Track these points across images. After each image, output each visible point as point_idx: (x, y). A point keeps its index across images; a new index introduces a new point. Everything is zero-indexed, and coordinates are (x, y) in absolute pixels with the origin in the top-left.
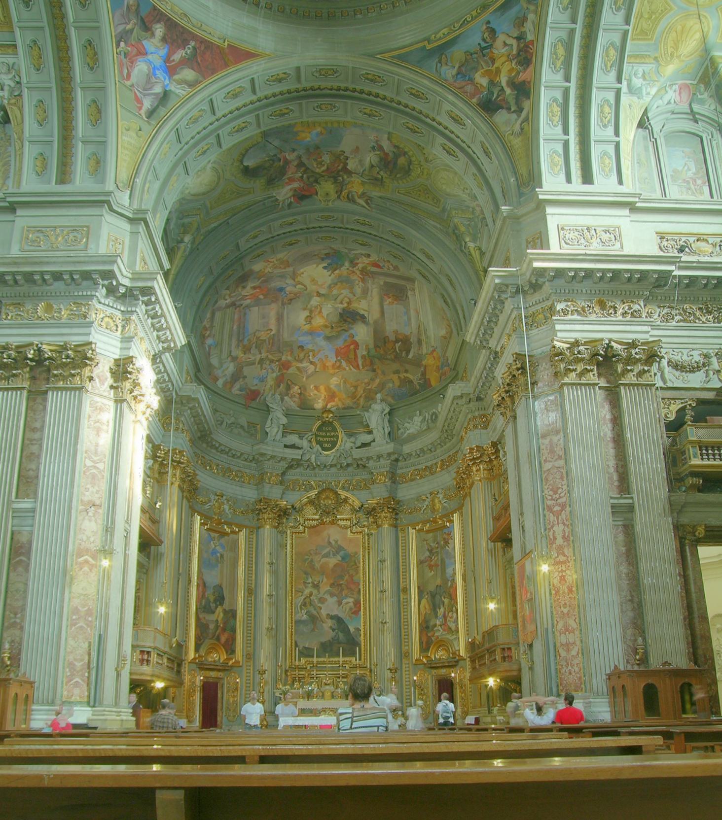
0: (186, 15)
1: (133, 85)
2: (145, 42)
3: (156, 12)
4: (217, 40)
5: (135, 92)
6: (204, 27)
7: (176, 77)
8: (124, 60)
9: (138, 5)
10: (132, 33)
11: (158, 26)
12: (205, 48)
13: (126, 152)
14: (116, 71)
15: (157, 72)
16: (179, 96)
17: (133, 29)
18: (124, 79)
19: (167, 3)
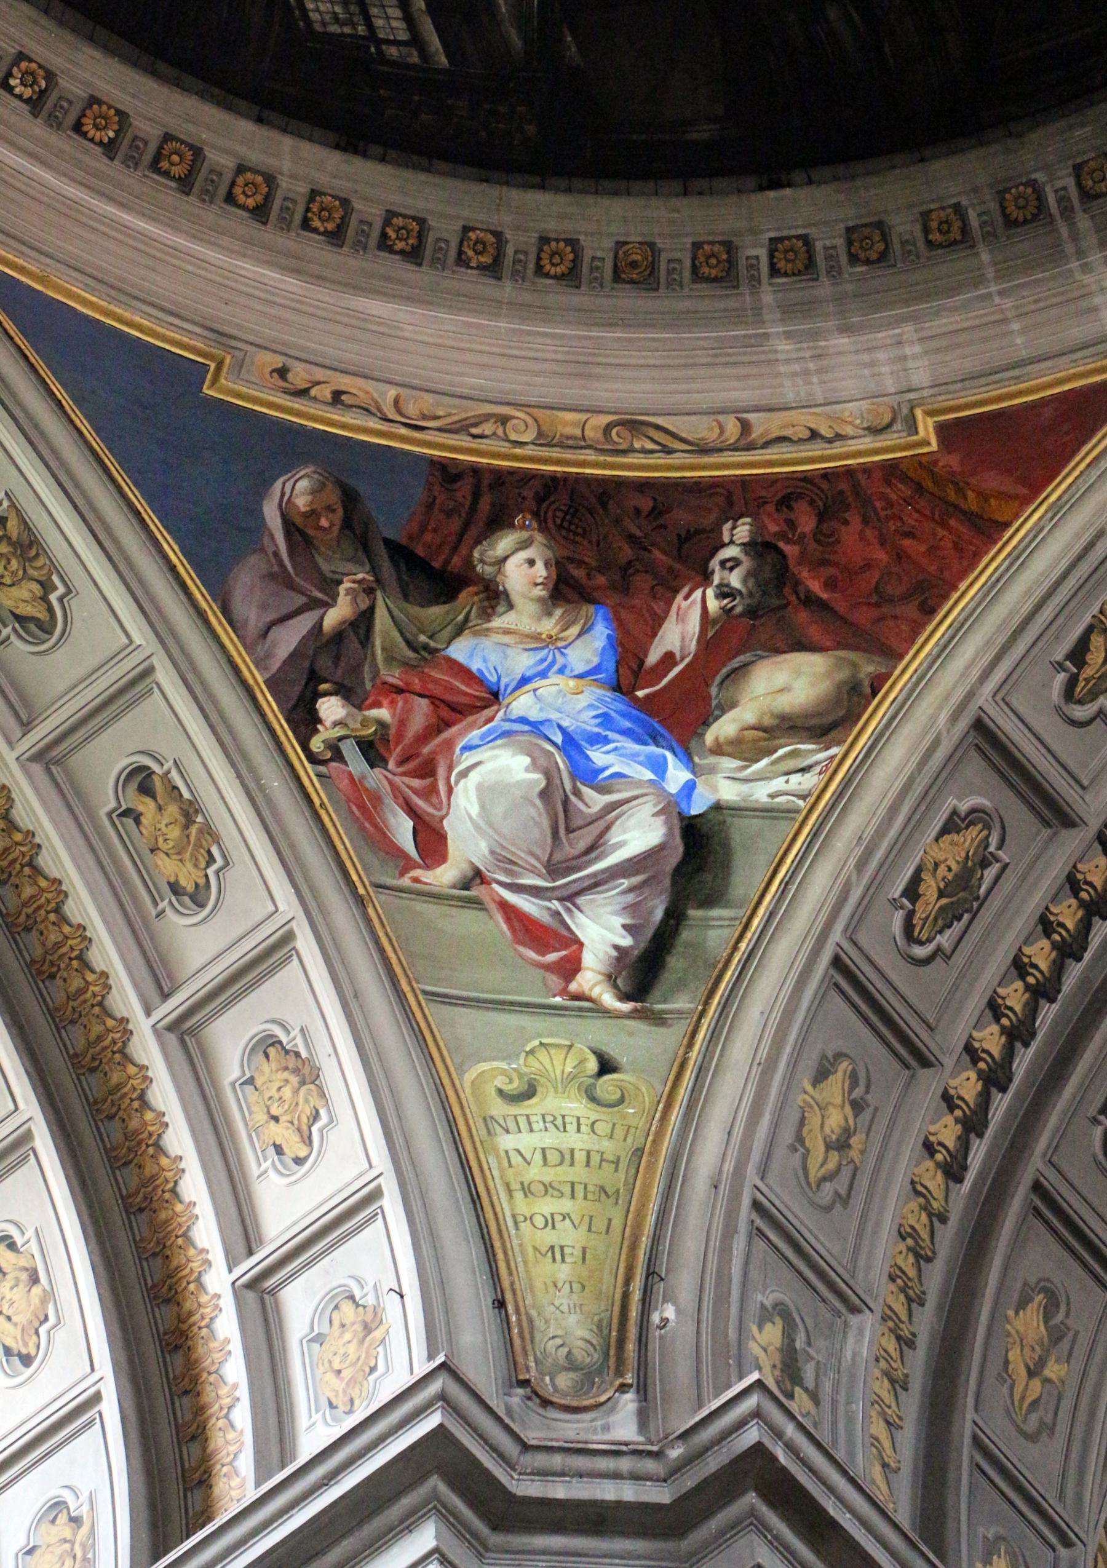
0: (634, 426)
1: (477, 877)
2: (460, 650)
3: (465, 488)
4: (867, 442)
5: (509, 911)
6: (763, 425)
7: (724, 728)
8: (375, 778)
9: (350, 498)
10: (366, 639)
11: (505, 543)
12: (822, 517)
13: (547, 1206)
14: (345, 843)
15: (598, 756)
16: (789, 812)
17: (370, 612)
18: (406, 864)
19: (504, 420)
